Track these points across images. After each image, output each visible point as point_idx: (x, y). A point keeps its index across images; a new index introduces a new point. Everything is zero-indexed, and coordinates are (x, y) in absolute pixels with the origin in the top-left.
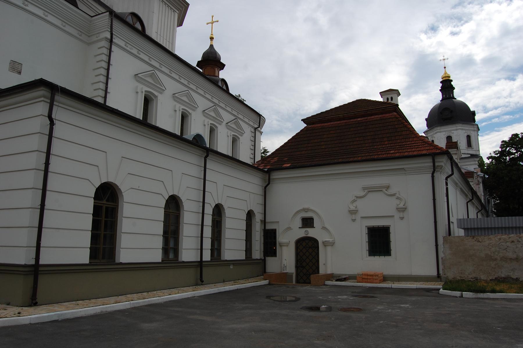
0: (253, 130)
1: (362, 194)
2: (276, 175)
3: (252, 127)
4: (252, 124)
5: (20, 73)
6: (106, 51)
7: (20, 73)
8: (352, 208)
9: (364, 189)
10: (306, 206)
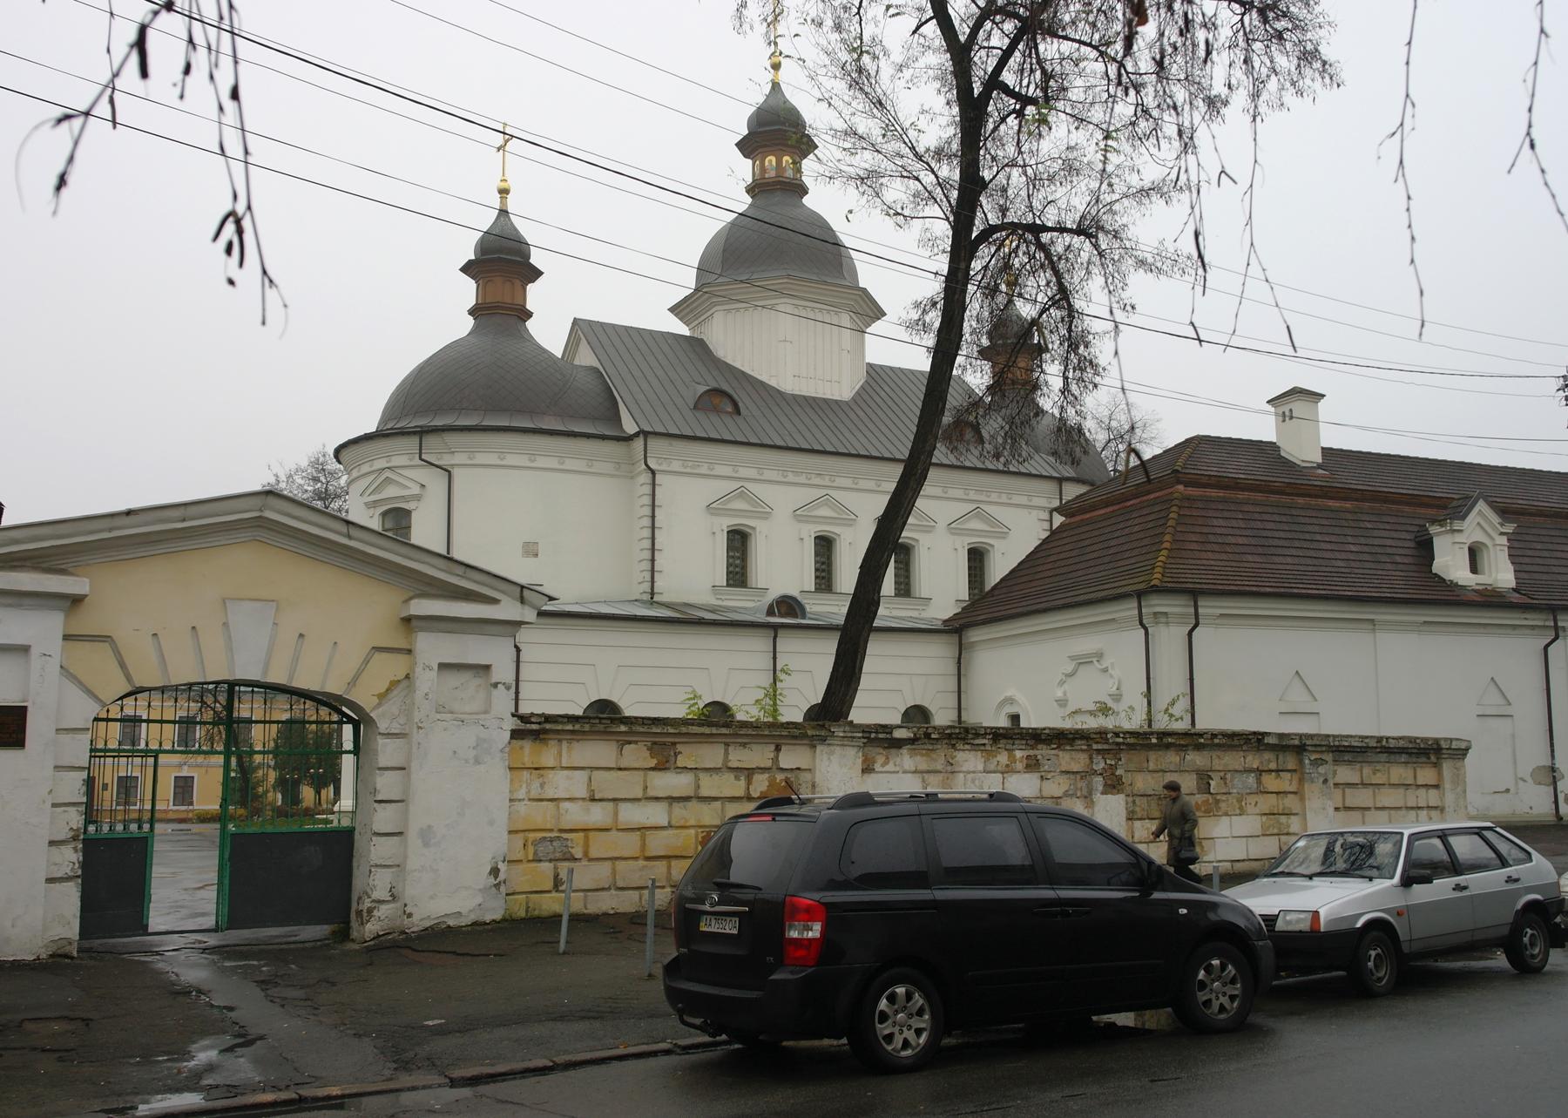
0: (1046, 516)
1: (1069, 669)
2: (975, 635)
3: (1043, 508)
4: (1037, 501)
5: (536, 555)
6: (647, 489)
7: (536, 555)
8: (1059, 694)
9: (1072, 658)
10: (1009, 694)
